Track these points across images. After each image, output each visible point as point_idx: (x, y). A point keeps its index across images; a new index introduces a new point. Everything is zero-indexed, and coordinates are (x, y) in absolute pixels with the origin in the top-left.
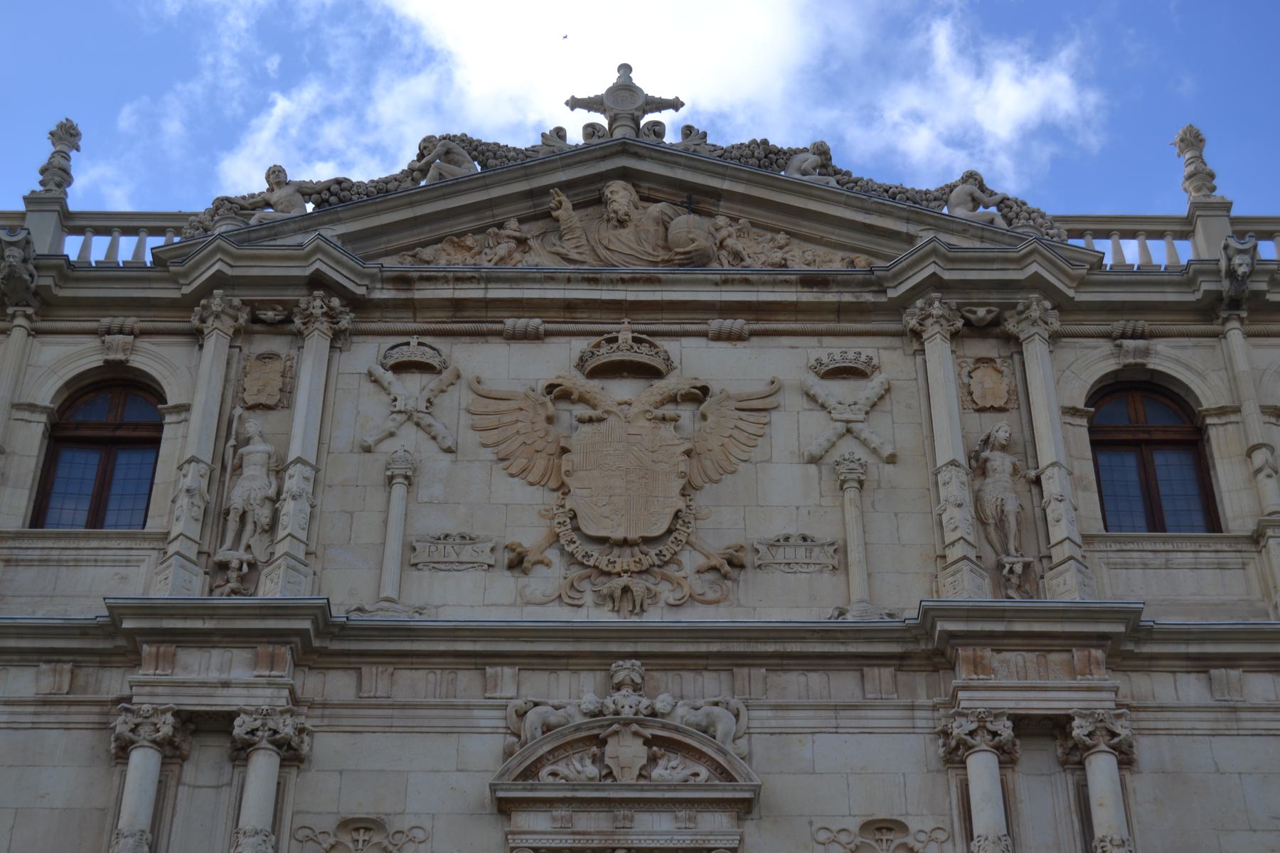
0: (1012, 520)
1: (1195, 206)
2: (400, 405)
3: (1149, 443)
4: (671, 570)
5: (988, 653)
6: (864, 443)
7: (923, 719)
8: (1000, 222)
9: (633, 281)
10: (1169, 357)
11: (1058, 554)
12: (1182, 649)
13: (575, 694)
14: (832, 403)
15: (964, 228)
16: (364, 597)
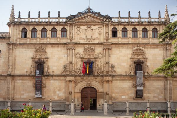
10: (116, 27)
13: (87, 46)
16: (77, 41)
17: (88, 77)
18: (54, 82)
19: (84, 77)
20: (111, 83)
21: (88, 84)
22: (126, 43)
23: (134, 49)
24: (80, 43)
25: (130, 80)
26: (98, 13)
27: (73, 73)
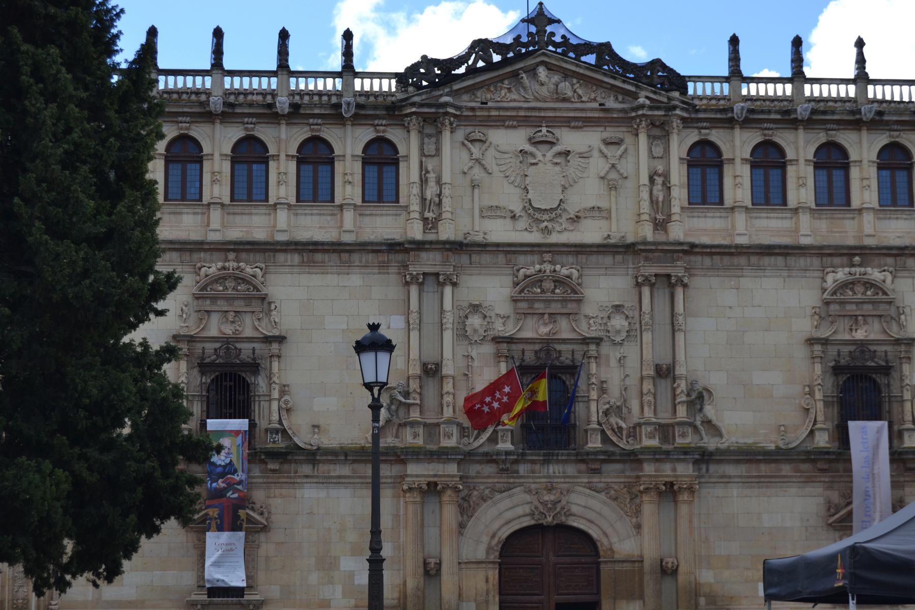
0: (661, 204)
2: (474, 157)
7: (631, 272)
11: (674, 218)
14: (609, 155)
17: (547, 462)
18: (322, 494)
19: (516, 462)
20: (690, 503)
21: (544, 504)
22: (780, 247)
23: (830, 278)
24: (486, 245)
25: (809, 480)
26: (601, 45)
27: (449, 436)
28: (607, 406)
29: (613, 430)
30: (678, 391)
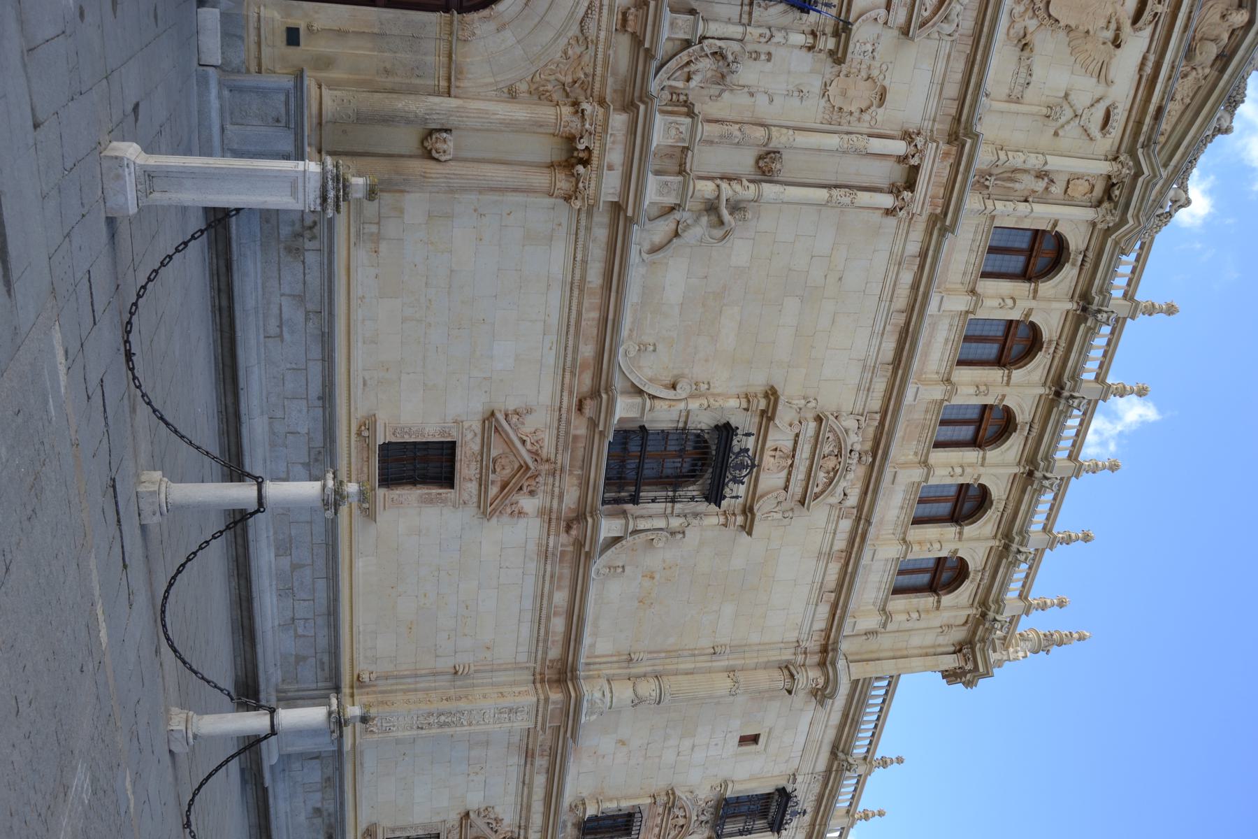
0: (1011, 185)
1: (1138, 303)
3: (1030, 256)
4: (1030, 13)
5: (951, 161)
6: (1068, 122)
8: (1160, 211)
9: (1189, 18)
10: (1068, 275)
11: (989, 203)
12: (932, 248)
14: (1093, 110)
15: (1162, 193)
28: (730, 58)
29: (688, 63)
30: (737, 187)
